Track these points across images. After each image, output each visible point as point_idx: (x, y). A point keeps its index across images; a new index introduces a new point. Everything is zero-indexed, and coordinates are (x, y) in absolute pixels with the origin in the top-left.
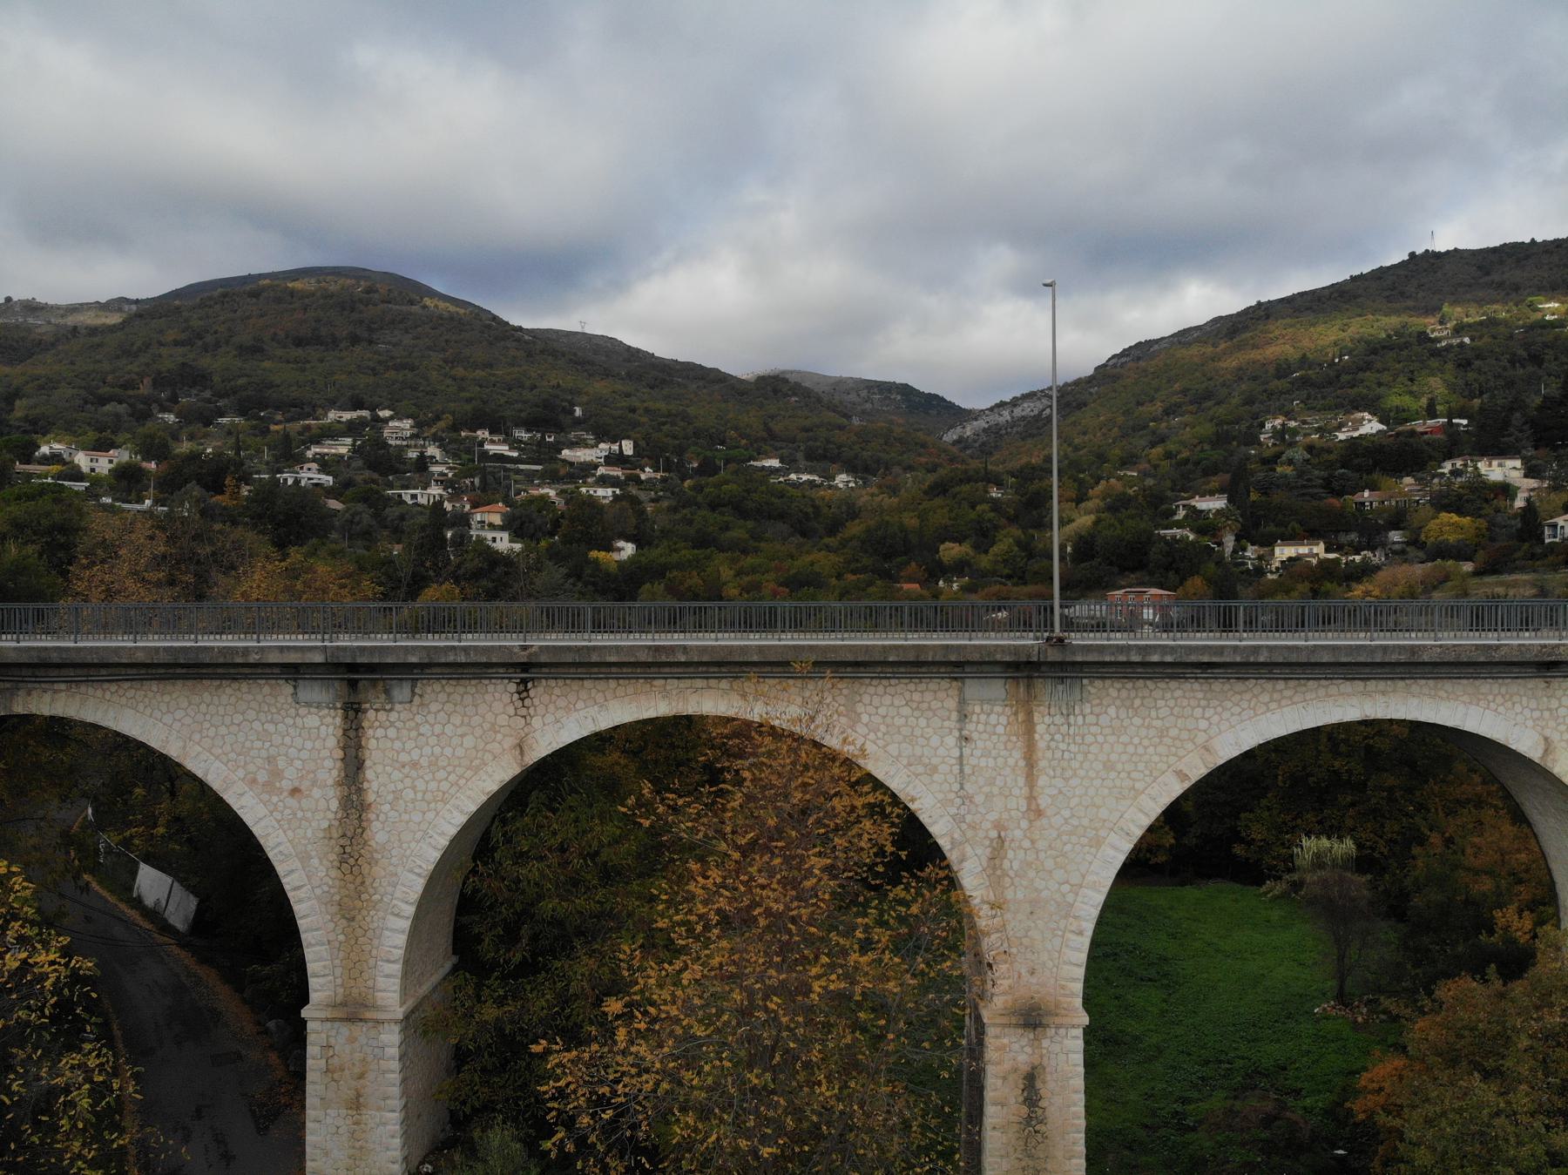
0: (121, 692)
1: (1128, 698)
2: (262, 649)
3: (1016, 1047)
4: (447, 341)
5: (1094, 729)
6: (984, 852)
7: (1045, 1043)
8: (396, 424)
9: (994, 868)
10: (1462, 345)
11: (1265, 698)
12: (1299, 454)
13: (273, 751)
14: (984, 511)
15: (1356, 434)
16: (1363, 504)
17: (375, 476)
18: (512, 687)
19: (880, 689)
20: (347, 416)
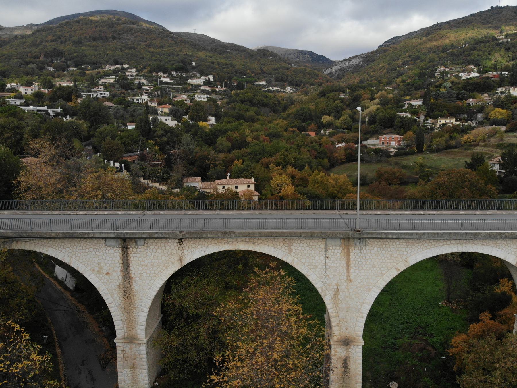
0: (48, 242)
1: (381, 245)
2: (94, 233)
3: (341, 351)
4: (146, 38)
5: (369, 254)
6: (332, 293)
7: (350, 350)
8: (130, 70)
9: (335, 298)
10: (507, 42)
11: (426, 245)
12: (448, 84)
13: (99, 261)
14: (338, 103)
15: (469, 77)
16: (469, 104)
17: (124, 91)
18: (177, 241)
19: (299, 241)
20: (113, 67)
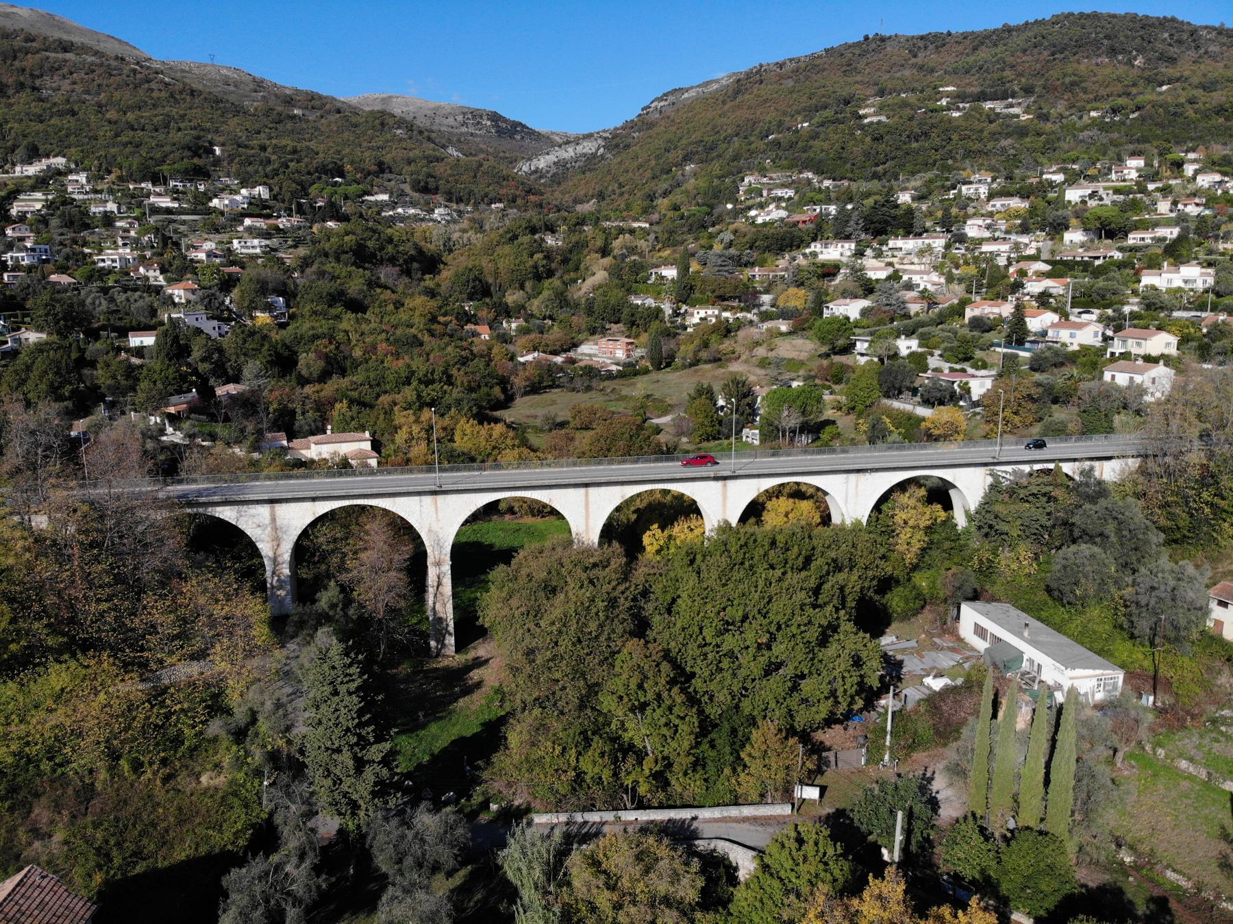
8: (75, 178)
20: (32, 170)
